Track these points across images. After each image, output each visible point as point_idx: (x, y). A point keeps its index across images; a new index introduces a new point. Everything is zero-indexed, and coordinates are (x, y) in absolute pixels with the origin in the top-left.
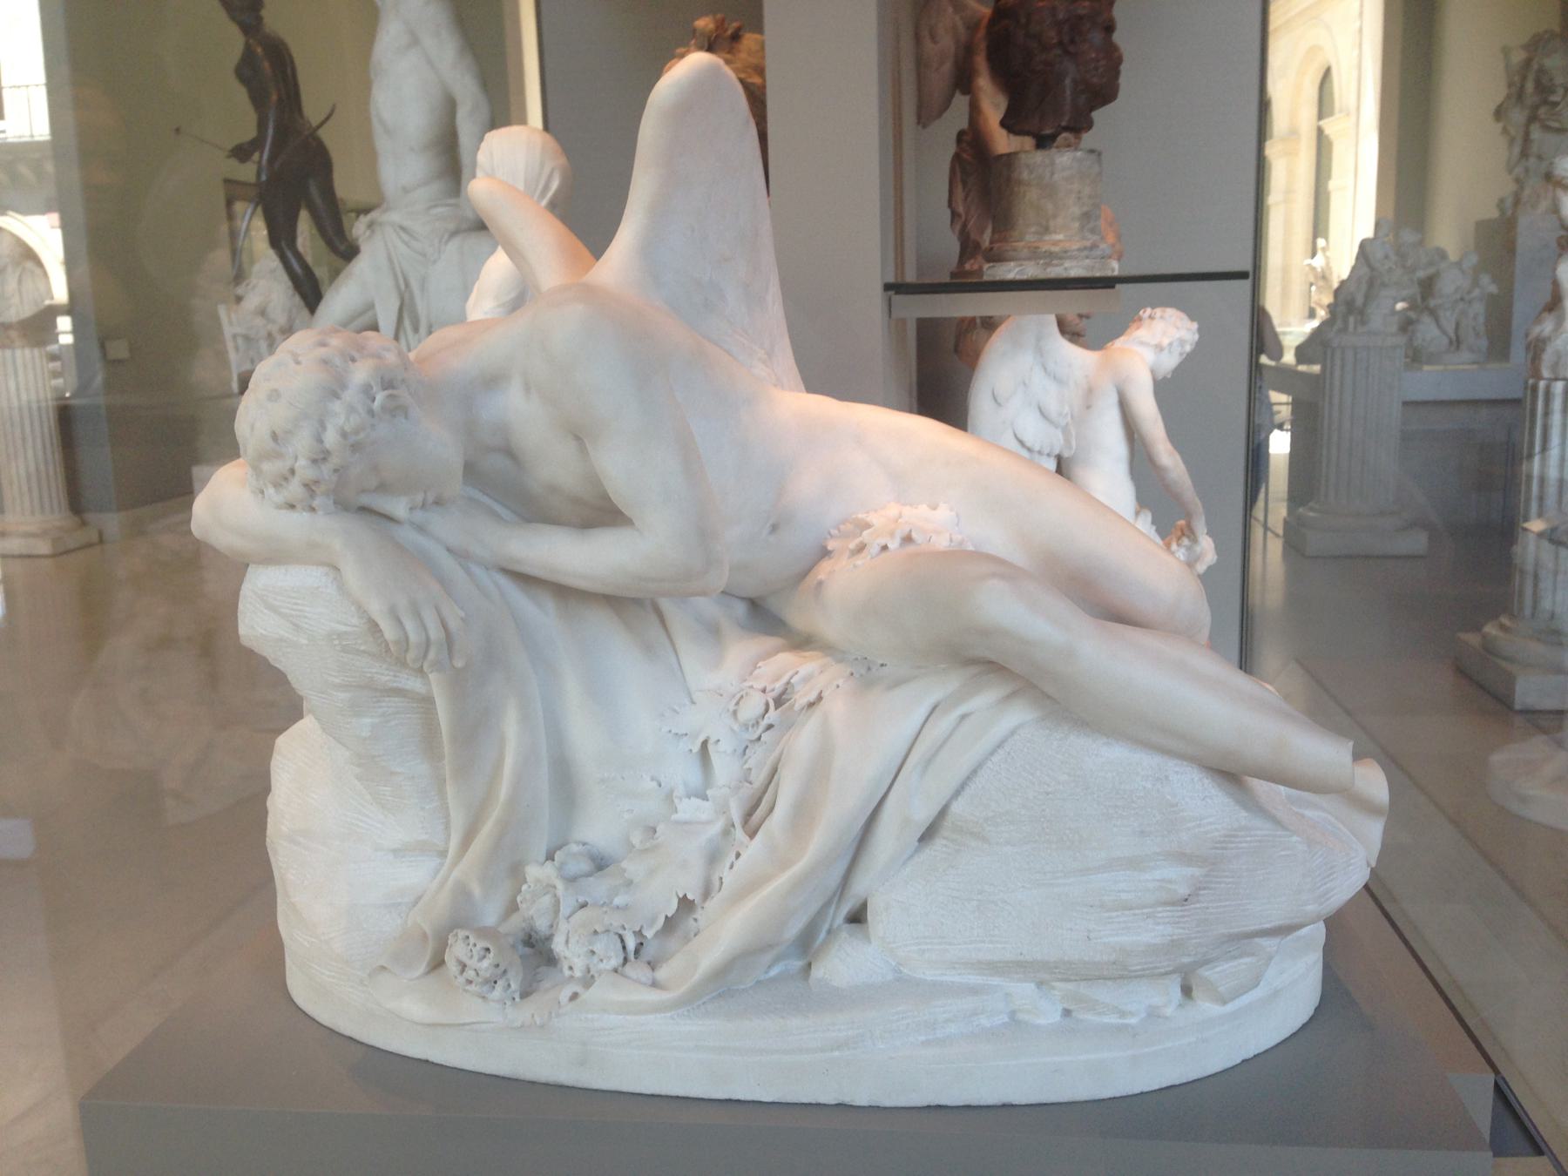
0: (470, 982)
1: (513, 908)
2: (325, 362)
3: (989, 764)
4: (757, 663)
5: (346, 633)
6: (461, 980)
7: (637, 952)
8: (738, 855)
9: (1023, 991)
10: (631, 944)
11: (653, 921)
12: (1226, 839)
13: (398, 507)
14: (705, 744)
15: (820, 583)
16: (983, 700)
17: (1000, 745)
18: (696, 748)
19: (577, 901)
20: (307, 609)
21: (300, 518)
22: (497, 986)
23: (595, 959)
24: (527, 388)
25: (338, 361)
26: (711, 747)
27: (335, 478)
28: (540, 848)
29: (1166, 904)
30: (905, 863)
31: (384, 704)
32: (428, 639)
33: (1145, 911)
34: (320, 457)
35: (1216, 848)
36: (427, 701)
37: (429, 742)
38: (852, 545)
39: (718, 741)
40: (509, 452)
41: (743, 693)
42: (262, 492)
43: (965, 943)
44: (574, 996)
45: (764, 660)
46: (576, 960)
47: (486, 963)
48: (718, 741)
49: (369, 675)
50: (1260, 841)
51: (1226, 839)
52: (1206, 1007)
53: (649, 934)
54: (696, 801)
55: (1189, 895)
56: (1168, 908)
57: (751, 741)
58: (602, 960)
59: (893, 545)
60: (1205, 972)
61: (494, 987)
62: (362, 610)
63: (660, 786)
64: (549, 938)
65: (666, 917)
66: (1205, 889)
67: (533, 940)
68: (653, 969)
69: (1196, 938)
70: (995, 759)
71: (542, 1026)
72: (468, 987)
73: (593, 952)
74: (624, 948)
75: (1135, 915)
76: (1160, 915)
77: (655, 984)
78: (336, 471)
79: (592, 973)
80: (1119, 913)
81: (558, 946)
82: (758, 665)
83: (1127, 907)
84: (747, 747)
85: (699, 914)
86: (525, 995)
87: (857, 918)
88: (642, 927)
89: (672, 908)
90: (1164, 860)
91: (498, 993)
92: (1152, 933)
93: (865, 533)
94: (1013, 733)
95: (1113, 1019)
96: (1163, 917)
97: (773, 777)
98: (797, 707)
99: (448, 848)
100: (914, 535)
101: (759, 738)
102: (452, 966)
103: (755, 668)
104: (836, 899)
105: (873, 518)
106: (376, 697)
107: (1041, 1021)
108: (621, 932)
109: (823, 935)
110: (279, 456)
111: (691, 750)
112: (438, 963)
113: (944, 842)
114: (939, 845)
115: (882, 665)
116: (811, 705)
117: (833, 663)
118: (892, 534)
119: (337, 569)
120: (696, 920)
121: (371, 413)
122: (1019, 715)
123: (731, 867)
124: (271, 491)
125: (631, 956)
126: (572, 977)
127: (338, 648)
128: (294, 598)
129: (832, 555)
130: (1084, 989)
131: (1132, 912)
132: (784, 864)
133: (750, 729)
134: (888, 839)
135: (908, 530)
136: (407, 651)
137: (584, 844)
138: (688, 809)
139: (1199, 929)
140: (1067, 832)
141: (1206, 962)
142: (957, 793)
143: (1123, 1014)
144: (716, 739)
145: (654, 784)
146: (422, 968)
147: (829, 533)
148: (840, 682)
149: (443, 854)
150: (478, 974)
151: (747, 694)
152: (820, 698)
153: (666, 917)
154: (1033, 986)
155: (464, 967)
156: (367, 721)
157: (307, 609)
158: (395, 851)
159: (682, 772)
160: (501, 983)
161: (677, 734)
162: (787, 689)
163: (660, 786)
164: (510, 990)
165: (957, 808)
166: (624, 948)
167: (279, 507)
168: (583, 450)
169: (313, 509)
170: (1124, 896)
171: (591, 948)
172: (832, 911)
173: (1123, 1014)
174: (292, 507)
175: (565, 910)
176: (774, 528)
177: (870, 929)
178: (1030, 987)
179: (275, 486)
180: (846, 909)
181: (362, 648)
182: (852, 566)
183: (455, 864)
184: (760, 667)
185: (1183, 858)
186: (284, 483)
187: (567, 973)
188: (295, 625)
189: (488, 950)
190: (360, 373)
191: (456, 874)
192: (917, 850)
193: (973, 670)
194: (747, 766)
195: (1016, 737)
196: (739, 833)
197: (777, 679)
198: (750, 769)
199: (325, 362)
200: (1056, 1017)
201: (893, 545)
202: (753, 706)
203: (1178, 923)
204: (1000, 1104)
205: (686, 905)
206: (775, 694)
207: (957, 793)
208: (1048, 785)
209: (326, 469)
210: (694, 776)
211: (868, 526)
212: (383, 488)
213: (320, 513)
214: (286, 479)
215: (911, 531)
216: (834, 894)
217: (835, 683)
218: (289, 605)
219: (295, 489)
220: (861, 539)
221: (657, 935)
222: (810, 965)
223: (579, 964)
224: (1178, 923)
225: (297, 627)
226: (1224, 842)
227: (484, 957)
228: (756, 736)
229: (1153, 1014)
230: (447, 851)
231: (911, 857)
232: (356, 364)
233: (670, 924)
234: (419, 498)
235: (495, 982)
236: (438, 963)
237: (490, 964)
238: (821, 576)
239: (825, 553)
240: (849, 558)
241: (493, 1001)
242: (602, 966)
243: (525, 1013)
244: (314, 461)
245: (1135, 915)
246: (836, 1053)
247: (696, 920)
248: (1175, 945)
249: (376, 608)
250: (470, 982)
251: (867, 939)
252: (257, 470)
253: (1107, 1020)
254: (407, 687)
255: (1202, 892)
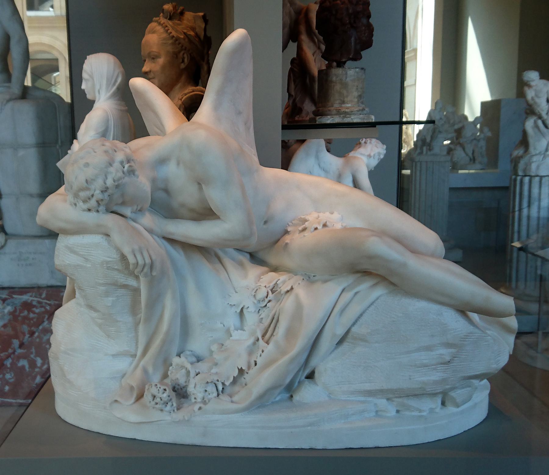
0: (157, 404)
1: (165, 376)
2: (106, 152)
3: (368, 311)
4: (261, 277)
5: (110, 261)
6: (153, 403)
7: (222, 392)
8: (263, 351)
9: (382, 402)
10: (220, 387)
11: (228, 379)
12: (469, 335)
13: (127, 211)
14: (242, 309)
15: (287, 244)
16: (365, 285)
17: (372, 304)
18: (239, 310)
19: (196, 372)
20: (93, 252)
21: (93, 215)
22: (168, 405)
23: (207, 393)
24: (178, 164)
25: (110, 152)
26: (245, 310)
27: (108, 198)
28: (175, 350)
29: (442, 364)
30: (331, 353)
31: (118, 292)
32: (137, 263)
33: (433, 367)
34: (104, 190)
35: (461, 341)
36: (136, 291)
37: (134, 309)
38: (300, 228)
39: (248, 307)
40: (166, 191)
41: (258, 288)
42: (75, 205)
43: (359, 383)
44: (200, 408)
45: (263, 275)
46: (199, 394)
47: (165, 395)
48: (248, 307)
49: (116, 279)
50: (477, 338)
51: (469, 335)
52: (451, 409)
53: (227, 383)
54: (240, 332)
55: (450, 360)
56: (442, 366)
57: (261, 307)
58: (209, 394)
59: (320, 227)
60: (452, 394)
61: (166, 406)
62: (118, 249)
63: (224, 326)
64: (185, 387)
65: (234, 377)
66: (456, 357)
67: (176, 389)
68: (231, 398)
69: (452, 378)
70: (370, 309)
71: (188, 421)
72: (156, 406)
73: (206, 391)
74: (217, 390)
75: (429, 369)
76: (438, 368)
77: (232, 402)
78: (109, 195)
79: (205, 400)
80: (422, 368)
81: (191, 389)
82: (261, 277)
83: (426, 366)
84: (260, 310)
85: (246, 376)
86: (178, 409)
87: (311, 376)
88: (224, 381)
89: (236, 373)
90: (440, 346)
91: (168, 408)
92: (436, 376)
93: (306, 223)
94: (377, 299)
95: (416, 413)
96: (439, 369)
97: (272, 321)
98: (282, 292)
99: (137, 353)
100: (328, 223)
101: (266, 305)
102: (147, 397)
103: (260, 278)
104: (302, 369)
105: (307, 217)
106: (115, 289)
107: (389, 415)
108: (217, 382)
109: (296, 384)
110: (88, 189)
111: (236, 312)
112: (140, 396)
113: (348, 344)
114: (345, 346)
115: (314, 276)
116: (288, 291)
117: (293, 276)
118: (319, 223)
119: (108, 235)
120: (244, 378)
121: (123, 172)
122: (380, 291)
123: (260, 356)
124: (81, 204)
125: (220, 393)
126: (196, 402)
127: (105, 268)
128: (87, 247)
129: (290, 233)
130: (406, 401)
131: (428, 367)
132: (283, 353)
133: (261, 302)
134: (326, 343)
135: (325, 221)
136: (136, 268)
137: (191, 351)
138: (236, 335)
139: (453, 374)
140: (401, 336)
141: (453, 389)
142: (354, 324)
143: (420, 411)
144: (248, 306)
145: (222, 325)
146: (133, 400)
147: (288, 224)
148: (300, 282)
149: (134, 356)
150: (161, 400)
151: (259, 288)
152: (292, 288)
153: (234, 377)
154: (385, 400)
155: (154, 397)
156: (110, 299)
157: (93, 252)
158: (113, 356)
159: (232, 321)
160: (170, 404)
161: (231, 305)
162: (274, 286)
163: (224, 326)
164: (173, 406)
165: (354, 329)
166: (217, 390)
167: (84, 210)
168: (200, 188)
169: (98, 211)
170: (425, 361)
171: (206, 389)
172: (301, 373)
173: (420, 411)
174: (89, 210)
175: (192, 374)
176: (266, 222)
177: (316, 381)
178: (384, 401)
179: (83, 202)
180: (307, 371)
181: (116, 267)
182: (303, 236)
183: (140, 360)
184: (262, 278)
185: (448, 345)
186: (88, 200)
187: (193, 400)
188: (85, 258)
189: (165, 390)
190: (120, 157)
191: (142, 363)
192: (336, 348)
193: (359, 275)
194: (261, 317)
195: (379, 300)
196: (261, 342)
197: (270, 282)
198: (262, 318)
199: (106, 152)
200: (394, 413)
201: (320, 227)
202: (262, 294)
203: (445, 371)
204: (374, 447)
205: (241, 371)
206: (271, 288)
207: (354, 324)
208: (394, 318)
209: (106, 194)
210: (237, 322)
211: (306, 221)
212: (123, 203)
213: (101, 213)
214: (89, 199)
215: (326, 222)
216: (302, 367)
217: (298, 282)
218: (85, 251)
219: (93, 203)
220: (304, 225)
221: (230, 385)
222: (292, 396)
223: (200, 396)
224: (445, 371)
225: (87, 260)
226: (465, 338)
227: (164, 393)
228: (264, 305)
229: (432, 410)
230: (136, 355)
231: (333, 351)
232: (117, 153)
233: (235, 381)
234: (135, 207)
235: (167, 404)
236: (140, 396)
237: (167, 395)
238: (287, 241)
239: (286, 232)
240: (299, 233)
241: (166, 411)
242: (210, 397)
243: (179, 416)
244: (102, 192)
245: (429, 369)
246: (309, 428)
247: (244, 378)
248: (444, 381)
249: (127, 251)
250: (157, 404)
251: (316, 383)
252: (76, 196)
253: (414, 414)
254: (130, 284)
255: (455, 359)
